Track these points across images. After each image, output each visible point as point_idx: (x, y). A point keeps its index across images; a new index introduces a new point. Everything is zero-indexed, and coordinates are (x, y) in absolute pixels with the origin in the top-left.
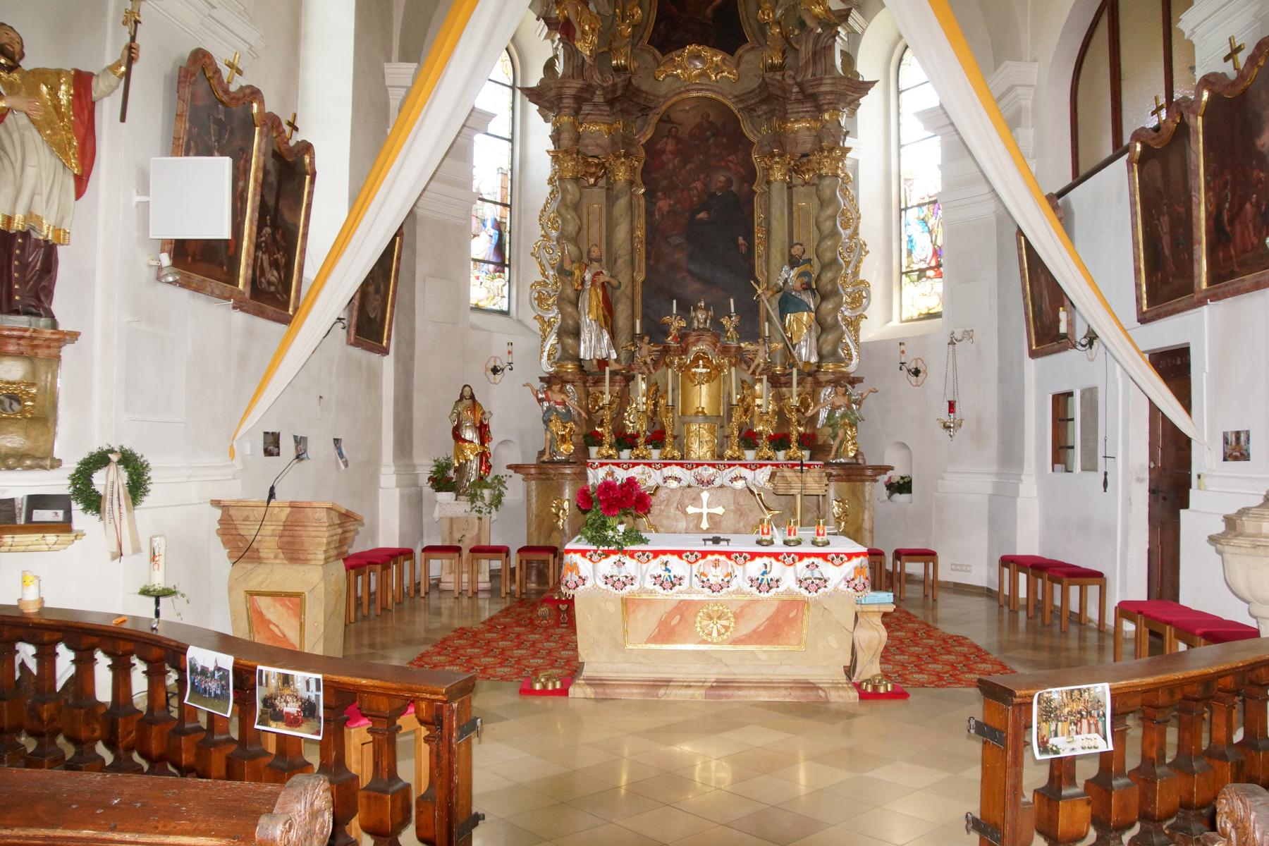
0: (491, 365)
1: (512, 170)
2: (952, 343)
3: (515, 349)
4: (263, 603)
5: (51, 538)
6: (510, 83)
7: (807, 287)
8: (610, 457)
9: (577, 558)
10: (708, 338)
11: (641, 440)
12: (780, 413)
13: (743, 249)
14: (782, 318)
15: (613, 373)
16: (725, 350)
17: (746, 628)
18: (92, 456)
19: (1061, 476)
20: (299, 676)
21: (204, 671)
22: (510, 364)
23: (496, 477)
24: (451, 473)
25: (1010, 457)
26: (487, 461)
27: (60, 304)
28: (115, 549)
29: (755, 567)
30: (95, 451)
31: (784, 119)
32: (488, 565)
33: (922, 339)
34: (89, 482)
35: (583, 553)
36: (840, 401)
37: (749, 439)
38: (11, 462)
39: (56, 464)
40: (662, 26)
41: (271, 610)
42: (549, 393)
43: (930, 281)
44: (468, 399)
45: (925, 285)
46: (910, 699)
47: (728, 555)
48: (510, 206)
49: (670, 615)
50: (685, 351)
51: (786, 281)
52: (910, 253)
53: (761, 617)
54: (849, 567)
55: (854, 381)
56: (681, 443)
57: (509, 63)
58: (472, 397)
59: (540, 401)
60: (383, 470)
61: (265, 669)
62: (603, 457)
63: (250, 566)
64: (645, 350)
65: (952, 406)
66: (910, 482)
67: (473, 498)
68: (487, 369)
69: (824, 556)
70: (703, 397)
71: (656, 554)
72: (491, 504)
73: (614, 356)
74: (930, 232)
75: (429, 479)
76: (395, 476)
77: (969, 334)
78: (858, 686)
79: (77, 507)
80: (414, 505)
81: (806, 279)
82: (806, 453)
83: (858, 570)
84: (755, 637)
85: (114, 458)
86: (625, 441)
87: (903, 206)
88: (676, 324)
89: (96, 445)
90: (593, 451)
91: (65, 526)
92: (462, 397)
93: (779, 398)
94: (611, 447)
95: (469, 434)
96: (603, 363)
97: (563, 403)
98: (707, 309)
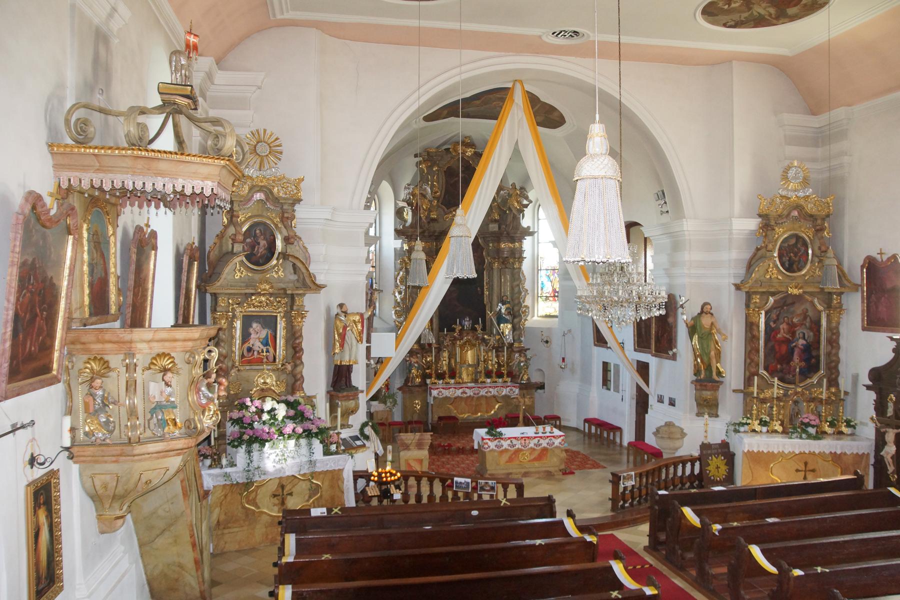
2: (564, 335)
7: (509, 313)
8: (435, 383)
9: (487, 441)
10: (471, 334)
11: (447, 376)
12: (498, 363)
13: (480, 293)
14: (499, 325)
15: (435, 348)
16: (477, 338)
17: (532, 457)
19: (605, 391)
20: (490, 482)
21: (461, 483)
25: (586, 379)
29: (536, 441)
31: (499, 242)
33: (549, 329)
35: (489, 439)
36: (522, 359)
37: (488, 374)
39: (352, 426)
40: (447, 196)
41: (413, 464)
42: (412, 359)
43: (551, 302)
45: (549, 303)
46: (576, 474)
47: (528, 437)
48: (374, 267)
49: (512, 455)
50: (462, 339)
51: (500, 310)
52: (542, 289)
53: (536, 454)
54: (560, 440)
55: (526, 350)
56: (461, 374)
61: (480, 481)
62: (432, 383)
64: (448, 340)
65: (563, 360)
66: (544, 385)
67: (385, 403)
69: (554, 437)
70: (470, 356)
71: (509, 438)
73: (434, 342)
74: (551, 282)
77: (570, 331)
78: (561, 470)
81: (509, 310)
82: (509, 379)
83: (563, 440)
84: (536, 459)
86: (441, 376)
87: (539, 268)
88: (458, 328)
90: (428, 381)
91: (364, 446)
93: (497, 356)
94: (435, 379)
96: (430, 345)
97: (417, 362)
98: (469, 320)
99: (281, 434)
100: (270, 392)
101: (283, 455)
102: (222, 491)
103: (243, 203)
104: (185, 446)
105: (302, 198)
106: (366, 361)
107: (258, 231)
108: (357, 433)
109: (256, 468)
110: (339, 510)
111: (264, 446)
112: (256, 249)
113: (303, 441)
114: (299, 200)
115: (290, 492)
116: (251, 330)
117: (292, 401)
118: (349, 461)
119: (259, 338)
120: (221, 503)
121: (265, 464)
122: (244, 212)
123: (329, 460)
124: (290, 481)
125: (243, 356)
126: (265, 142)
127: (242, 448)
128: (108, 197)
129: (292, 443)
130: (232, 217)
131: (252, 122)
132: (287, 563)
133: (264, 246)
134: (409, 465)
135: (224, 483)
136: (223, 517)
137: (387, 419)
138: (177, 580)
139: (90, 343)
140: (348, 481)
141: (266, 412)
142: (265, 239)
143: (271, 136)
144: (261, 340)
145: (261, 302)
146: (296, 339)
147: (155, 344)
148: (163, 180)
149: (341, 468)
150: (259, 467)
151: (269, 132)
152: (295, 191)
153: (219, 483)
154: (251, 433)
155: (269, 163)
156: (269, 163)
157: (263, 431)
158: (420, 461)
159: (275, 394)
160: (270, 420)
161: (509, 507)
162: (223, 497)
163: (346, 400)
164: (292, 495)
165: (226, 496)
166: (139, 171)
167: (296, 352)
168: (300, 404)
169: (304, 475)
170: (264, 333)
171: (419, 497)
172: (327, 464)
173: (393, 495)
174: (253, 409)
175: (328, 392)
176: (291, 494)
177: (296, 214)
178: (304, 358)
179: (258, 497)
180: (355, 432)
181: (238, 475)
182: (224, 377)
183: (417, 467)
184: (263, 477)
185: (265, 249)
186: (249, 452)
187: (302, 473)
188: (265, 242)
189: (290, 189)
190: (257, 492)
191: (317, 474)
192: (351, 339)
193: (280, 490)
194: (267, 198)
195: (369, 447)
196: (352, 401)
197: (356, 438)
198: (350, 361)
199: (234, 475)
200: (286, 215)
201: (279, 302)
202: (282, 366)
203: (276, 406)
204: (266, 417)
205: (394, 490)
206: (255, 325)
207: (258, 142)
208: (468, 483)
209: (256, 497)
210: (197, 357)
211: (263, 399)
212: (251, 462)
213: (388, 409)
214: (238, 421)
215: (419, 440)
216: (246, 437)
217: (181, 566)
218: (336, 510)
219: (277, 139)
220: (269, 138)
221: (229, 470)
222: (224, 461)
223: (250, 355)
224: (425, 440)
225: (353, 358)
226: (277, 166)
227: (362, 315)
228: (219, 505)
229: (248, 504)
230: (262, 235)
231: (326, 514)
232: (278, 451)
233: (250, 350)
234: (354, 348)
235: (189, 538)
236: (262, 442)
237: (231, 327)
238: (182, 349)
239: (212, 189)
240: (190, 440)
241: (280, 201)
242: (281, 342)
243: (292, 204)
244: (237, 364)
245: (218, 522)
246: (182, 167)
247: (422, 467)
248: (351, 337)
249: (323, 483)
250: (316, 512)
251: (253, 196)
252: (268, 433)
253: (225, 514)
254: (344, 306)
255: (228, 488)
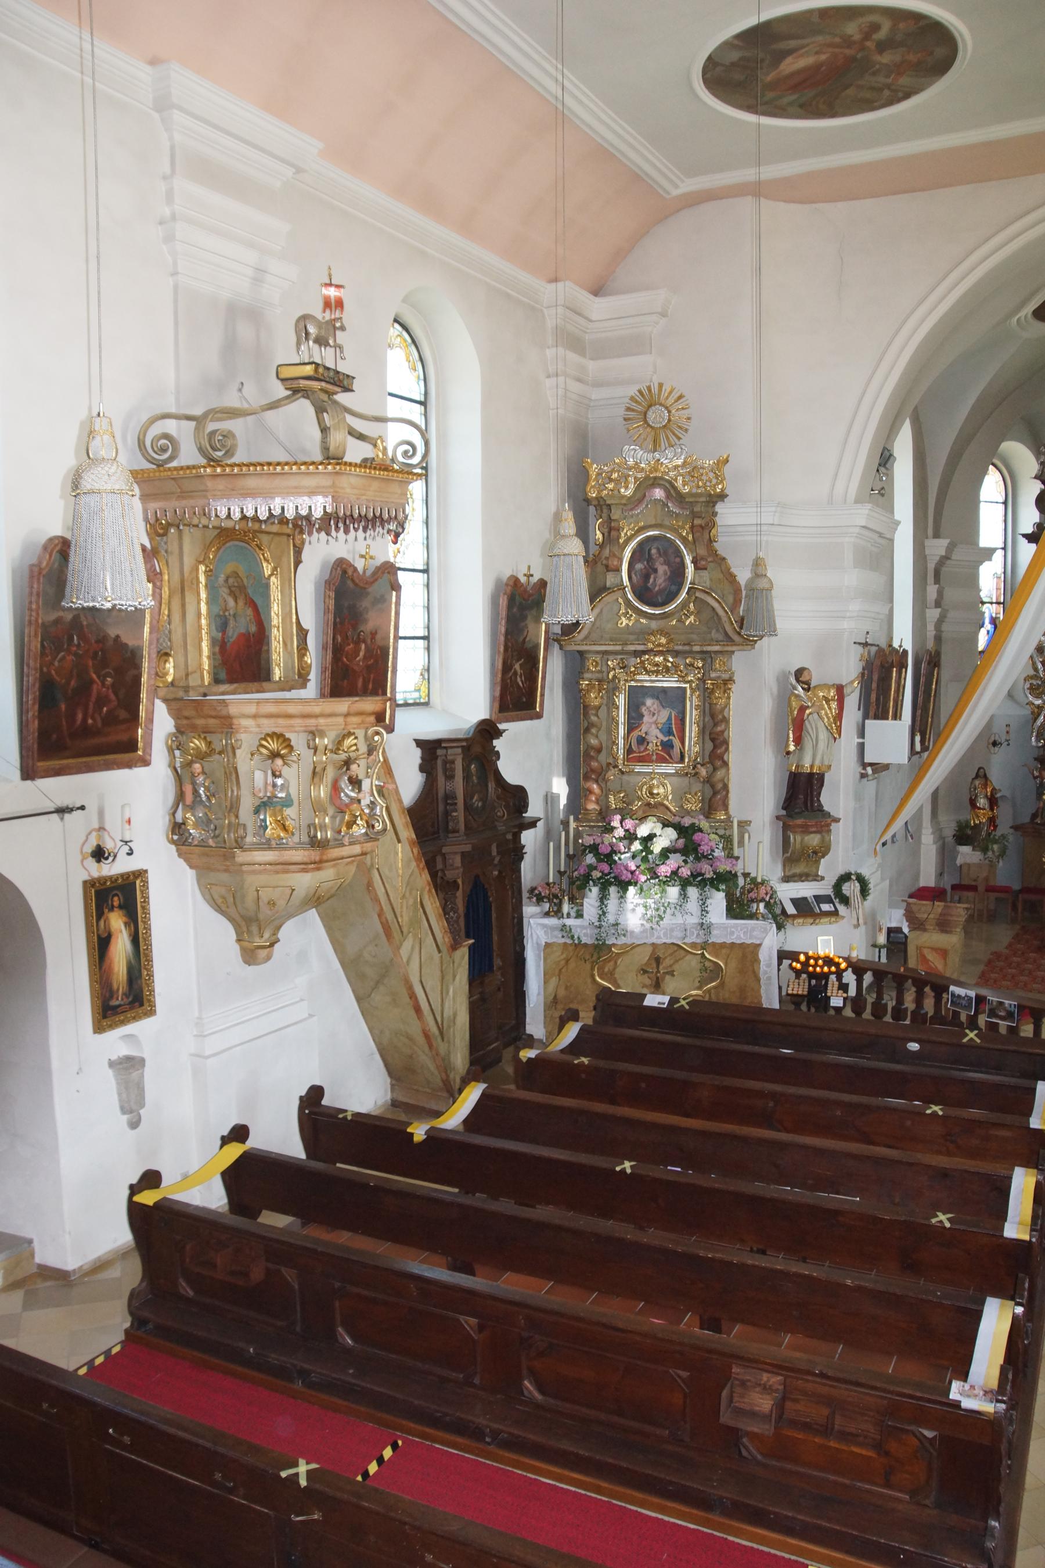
0: (991, 741)
1: (1005, 573)
3: (1012, 729)
4: (926, 952)
5: (833, 919)
6: (1002, 499)
18: (842, 876)
20: (1007, 1002)
21: (959, 996)
22: (1007, 741)
23: (1002, 835)
24: (969, 832)
26: (994, 822)
27: (827, 799)
28: (855, 922)
30: (843, 873)
32: (993, 896)
34: (841, 890)
38: (803, 879)
39: (823, 878)
41: (930, 956)
44: (981, 775)
57: (1002, 483)
58: (985, 776)
59: (1035, 778)
60: (924, 831)
63: (919, 932)
67: (985, 850)
68: (989, 744)
72: (1000, 855)
75: (954, 836)
76: (932, 836)
79: (836, 901)
80: (945, 855)
85: (853, 877)
89: (841, 870)
91: (835, 913)
92: (977, 776)
95: (982, 802)
99: (655, 875)
100: (662, 808)
101: (657, 910)
102: (562, 953)
103: (629, 507)
104: (305, 860)
105: (727, 492)
106: (860, 770)
107: (654, 551)
108: (829, 891)
109: (614, 925)
110: (687, 1003)
111: (625, 890)
112: (651, 580)
113: (693, 892)
114: (722, 496)
115: (669, 970)
116: (644, 710)
117: (686, 825)
118: (772, 931)
119: (656, 723)
120: (560, 970)
121: (627, 920)
122: (632, 520)
123: (736, 926)
124: (670, 951)
125: (629, 751)
126: (661, 405)
127: (590, 890)
128: (250, 524)
129: (673, 892)
130: (610, 529)
131: (655, 372)
132: (530, 1059)
133: (665, 573)
134: (924, 959)
135: (563, 940)
136: (562, 993)
137: (987, 879)
138: (411, 1057)
139: (193, 717)
140: (769, 965)
141: (639, 839)
142: (667, 563)
143: (670, 393)
144: (660, 726)
145: (657, 665)
146: (716, 725)
147: (265, 721)
148: (254, 502)
149: (758, 942)
150: (617, 924)
151: (667, 388)
152: (714, 481)
153: (554, 940)
154: (607, 869)
155: (668, 438)
156: (668, 438)
157: (626, 868)
158: (944, 953)
159: (669, 813)
160: (642, 851)
161: (978, 1047)
162: (563, 962)
163: (803, 832)
164: (673, 975)
165: (567, 961)
166: (219, 493)
167: (715, 747)
168: (700, 830)
169: (694, 945)
170: (664, 715)
171: (879, 1010)
172: (732, 933)
173: (829, 998)
174: (620, 832)
175: (778, 818)
176: (671, 973)
177: (718, 520)
178: (734, 756)
179: (617, 970)
180: (824, 888)
181: (584, 931)
182: (597, 781)
183: (937, 963)
184: (622, 940)
185: (665, 581)
186: (603, 898)
187: (688, 940)
188: (666, 567)
189: (704, 478)
190: (616, 963)
191: (717, 947)
192: (817, 729)
193: (654, 965)
194: (668, 496)
195: (843, 917)
196: (812, 835)
197: (819, 899)
198: (812, 766)
199: (579, 930)
200: (697, 522)
201: (692, 665)
202: (694, 769)
203: (658, 830)
204: (637, 846)
205: (835, 991)
206: (649, 702)
207: (650, 406)
208: (971, 998)
209: (614, 969)
210: (317, 740)
211: (642, 819)
212: (604, 913)
213: (987, 861)
214: (594, 848)
215: (941, 914)
216: (596, 874)
217: (410, 1038)
218: (683, 1003)
219: (681, 397)
220: (667, 398)
221: (569, 922)
222: (566, 908)
223: (642, 749)
224: (952, 916)
225: (817, 763)
226: (681, 442)
227: (840, 689)
228: (557, 971)
229: (601, 978)
230: (660, 555)
231: (665, 1006)
232: (650, 901)
233: (642, 741)
234: (822, 745)
235: (408, 999)
236: (623, 886)
237: (613, 705)
238: (302, 729)
239: (325, 507)
240: (312, 852)
241: (687, 500)
242: (692, 731)
243: (708, 502)
244: (620, 762)
245: (555, 996)
246: (277, 482)
247: (946, 965)
248: (817, 727)
249: (726, 964)
250: (653, 1000)
251: (645, 496)
252: (633, 873)
253: (567, 988)
254: (805, 673)
255: (571, 948)
